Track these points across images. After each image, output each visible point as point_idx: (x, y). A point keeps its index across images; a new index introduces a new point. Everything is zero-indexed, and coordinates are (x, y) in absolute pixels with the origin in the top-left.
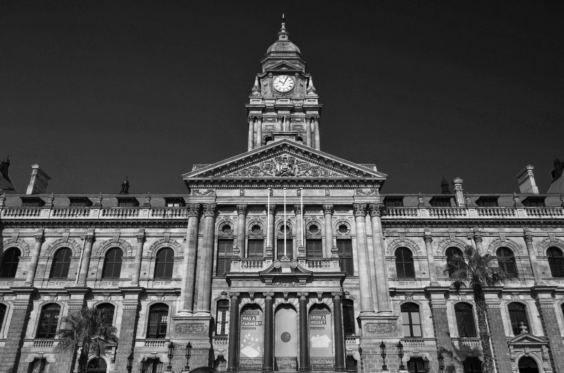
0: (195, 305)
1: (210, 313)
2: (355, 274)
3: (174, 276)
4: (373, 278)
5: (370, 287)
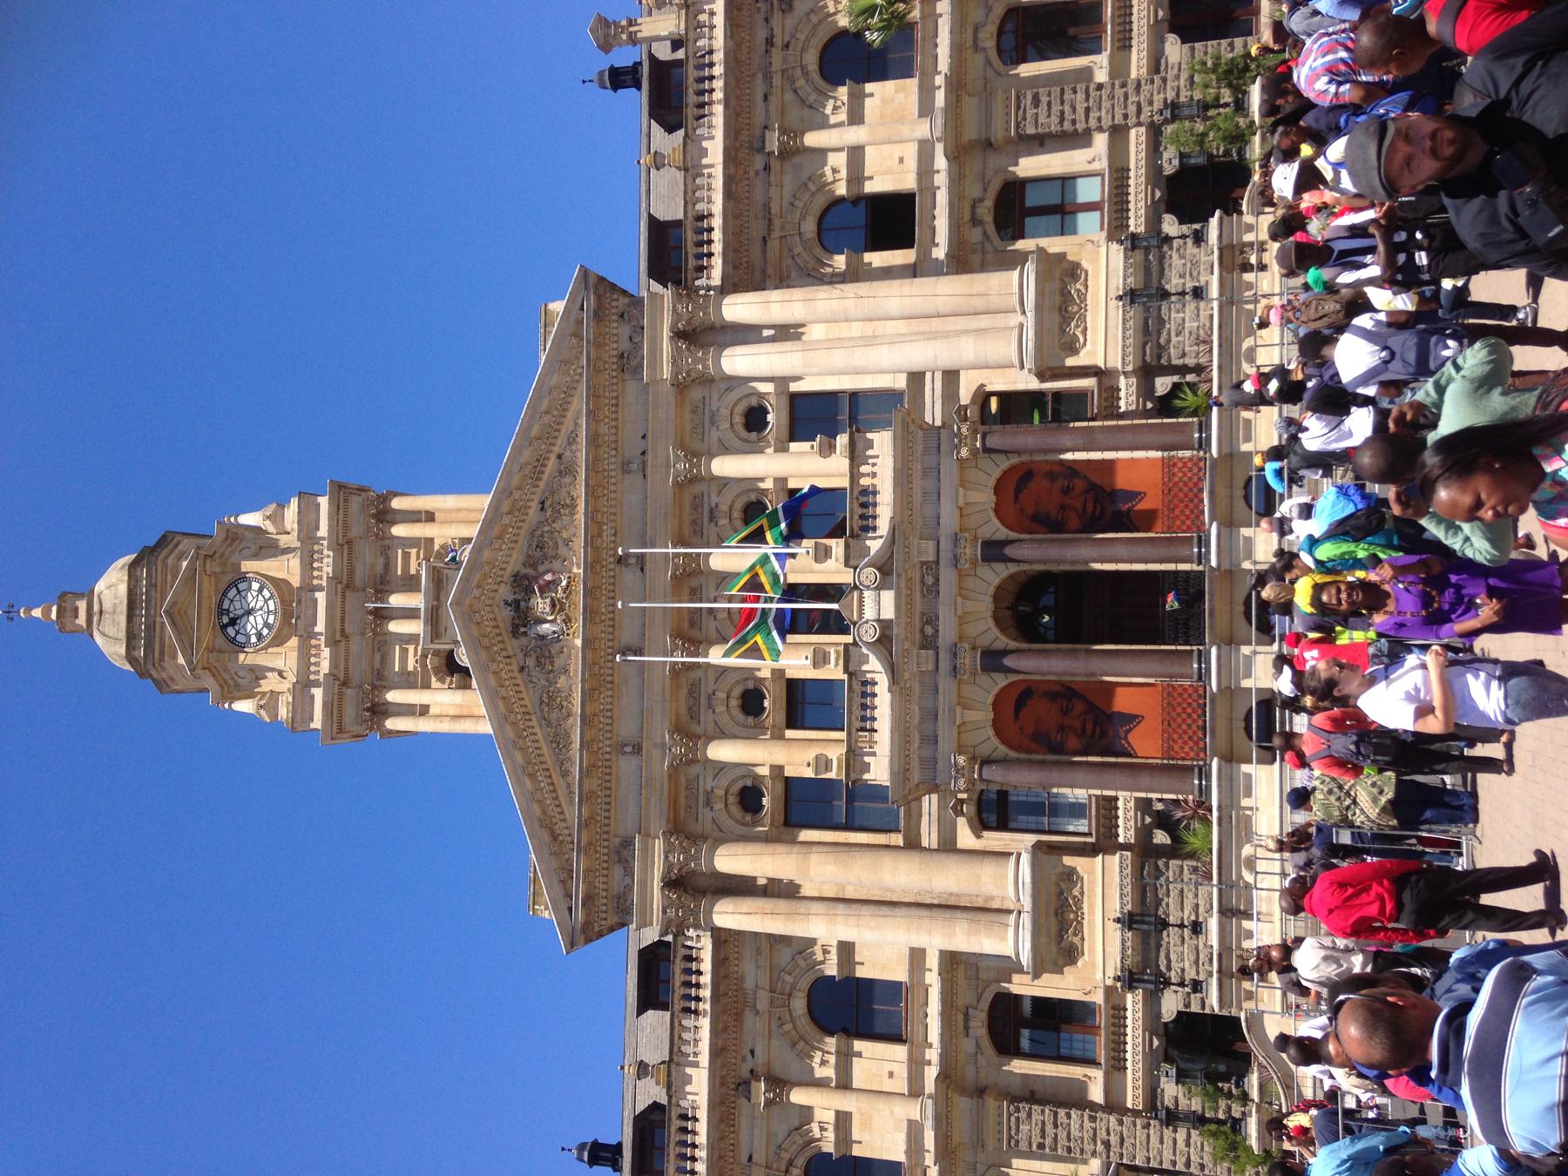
0: (995, 905)
1: (1019, 855)
2: (901, 383)
3: (900, 974)
4: (916, 325)
5: (946, 335)
